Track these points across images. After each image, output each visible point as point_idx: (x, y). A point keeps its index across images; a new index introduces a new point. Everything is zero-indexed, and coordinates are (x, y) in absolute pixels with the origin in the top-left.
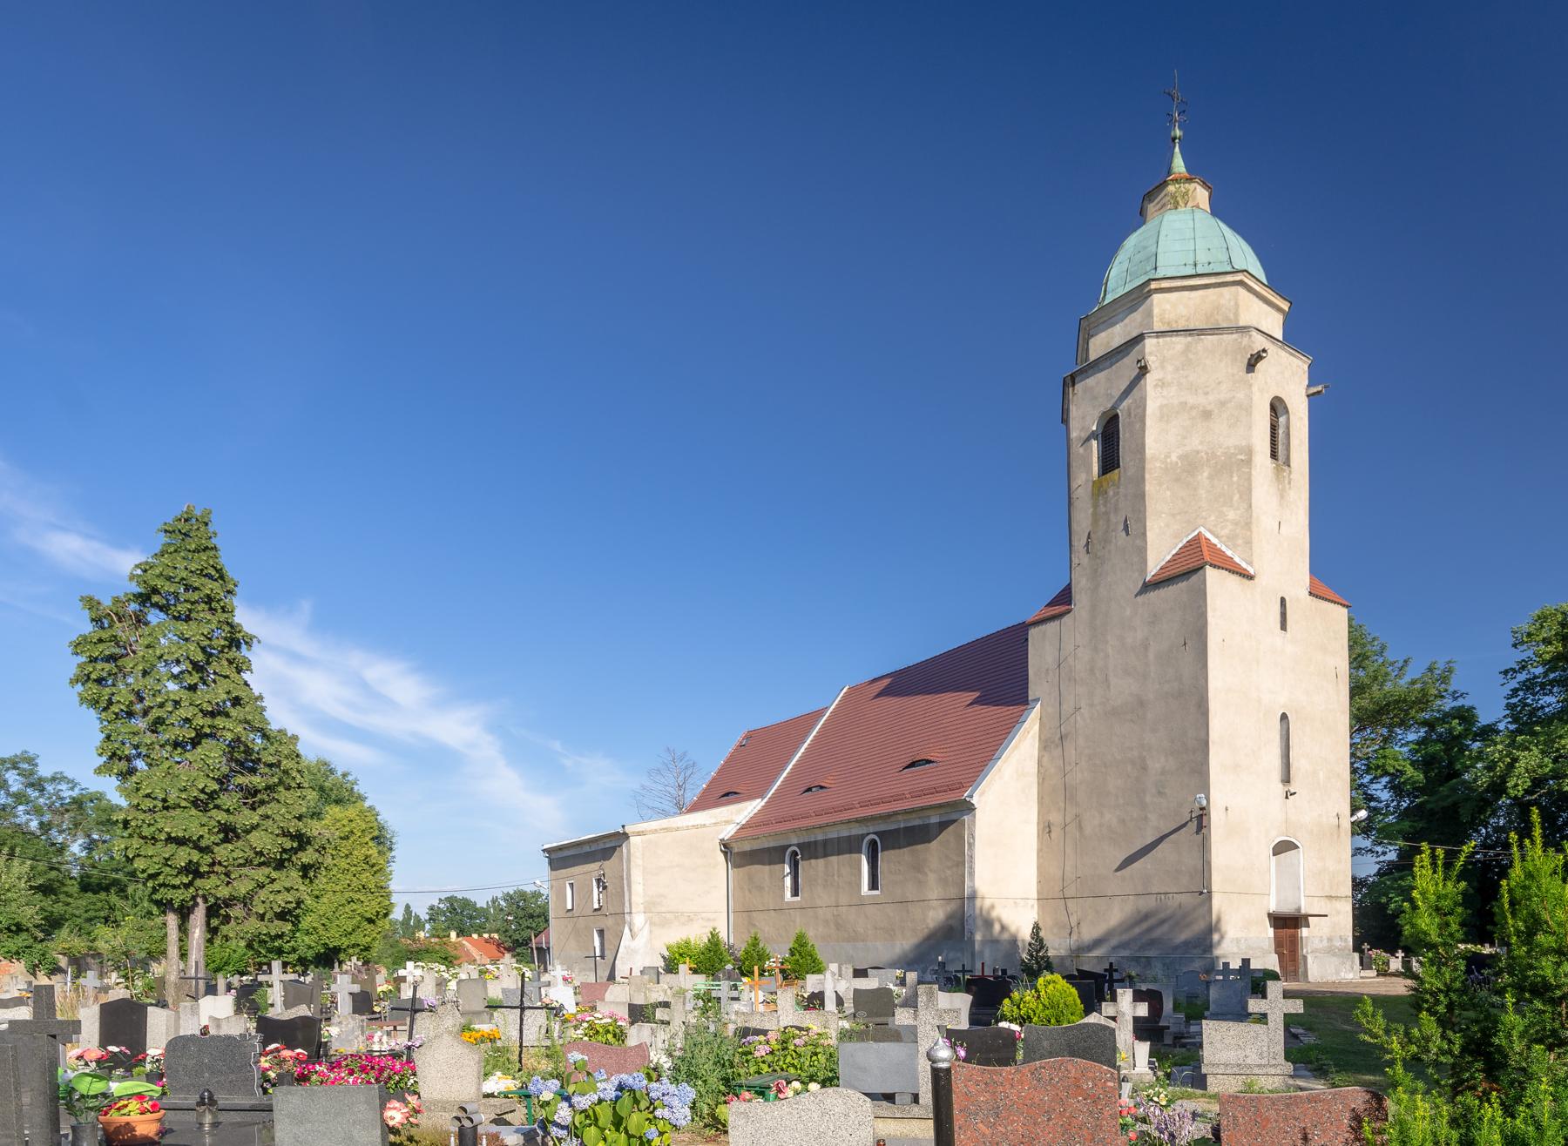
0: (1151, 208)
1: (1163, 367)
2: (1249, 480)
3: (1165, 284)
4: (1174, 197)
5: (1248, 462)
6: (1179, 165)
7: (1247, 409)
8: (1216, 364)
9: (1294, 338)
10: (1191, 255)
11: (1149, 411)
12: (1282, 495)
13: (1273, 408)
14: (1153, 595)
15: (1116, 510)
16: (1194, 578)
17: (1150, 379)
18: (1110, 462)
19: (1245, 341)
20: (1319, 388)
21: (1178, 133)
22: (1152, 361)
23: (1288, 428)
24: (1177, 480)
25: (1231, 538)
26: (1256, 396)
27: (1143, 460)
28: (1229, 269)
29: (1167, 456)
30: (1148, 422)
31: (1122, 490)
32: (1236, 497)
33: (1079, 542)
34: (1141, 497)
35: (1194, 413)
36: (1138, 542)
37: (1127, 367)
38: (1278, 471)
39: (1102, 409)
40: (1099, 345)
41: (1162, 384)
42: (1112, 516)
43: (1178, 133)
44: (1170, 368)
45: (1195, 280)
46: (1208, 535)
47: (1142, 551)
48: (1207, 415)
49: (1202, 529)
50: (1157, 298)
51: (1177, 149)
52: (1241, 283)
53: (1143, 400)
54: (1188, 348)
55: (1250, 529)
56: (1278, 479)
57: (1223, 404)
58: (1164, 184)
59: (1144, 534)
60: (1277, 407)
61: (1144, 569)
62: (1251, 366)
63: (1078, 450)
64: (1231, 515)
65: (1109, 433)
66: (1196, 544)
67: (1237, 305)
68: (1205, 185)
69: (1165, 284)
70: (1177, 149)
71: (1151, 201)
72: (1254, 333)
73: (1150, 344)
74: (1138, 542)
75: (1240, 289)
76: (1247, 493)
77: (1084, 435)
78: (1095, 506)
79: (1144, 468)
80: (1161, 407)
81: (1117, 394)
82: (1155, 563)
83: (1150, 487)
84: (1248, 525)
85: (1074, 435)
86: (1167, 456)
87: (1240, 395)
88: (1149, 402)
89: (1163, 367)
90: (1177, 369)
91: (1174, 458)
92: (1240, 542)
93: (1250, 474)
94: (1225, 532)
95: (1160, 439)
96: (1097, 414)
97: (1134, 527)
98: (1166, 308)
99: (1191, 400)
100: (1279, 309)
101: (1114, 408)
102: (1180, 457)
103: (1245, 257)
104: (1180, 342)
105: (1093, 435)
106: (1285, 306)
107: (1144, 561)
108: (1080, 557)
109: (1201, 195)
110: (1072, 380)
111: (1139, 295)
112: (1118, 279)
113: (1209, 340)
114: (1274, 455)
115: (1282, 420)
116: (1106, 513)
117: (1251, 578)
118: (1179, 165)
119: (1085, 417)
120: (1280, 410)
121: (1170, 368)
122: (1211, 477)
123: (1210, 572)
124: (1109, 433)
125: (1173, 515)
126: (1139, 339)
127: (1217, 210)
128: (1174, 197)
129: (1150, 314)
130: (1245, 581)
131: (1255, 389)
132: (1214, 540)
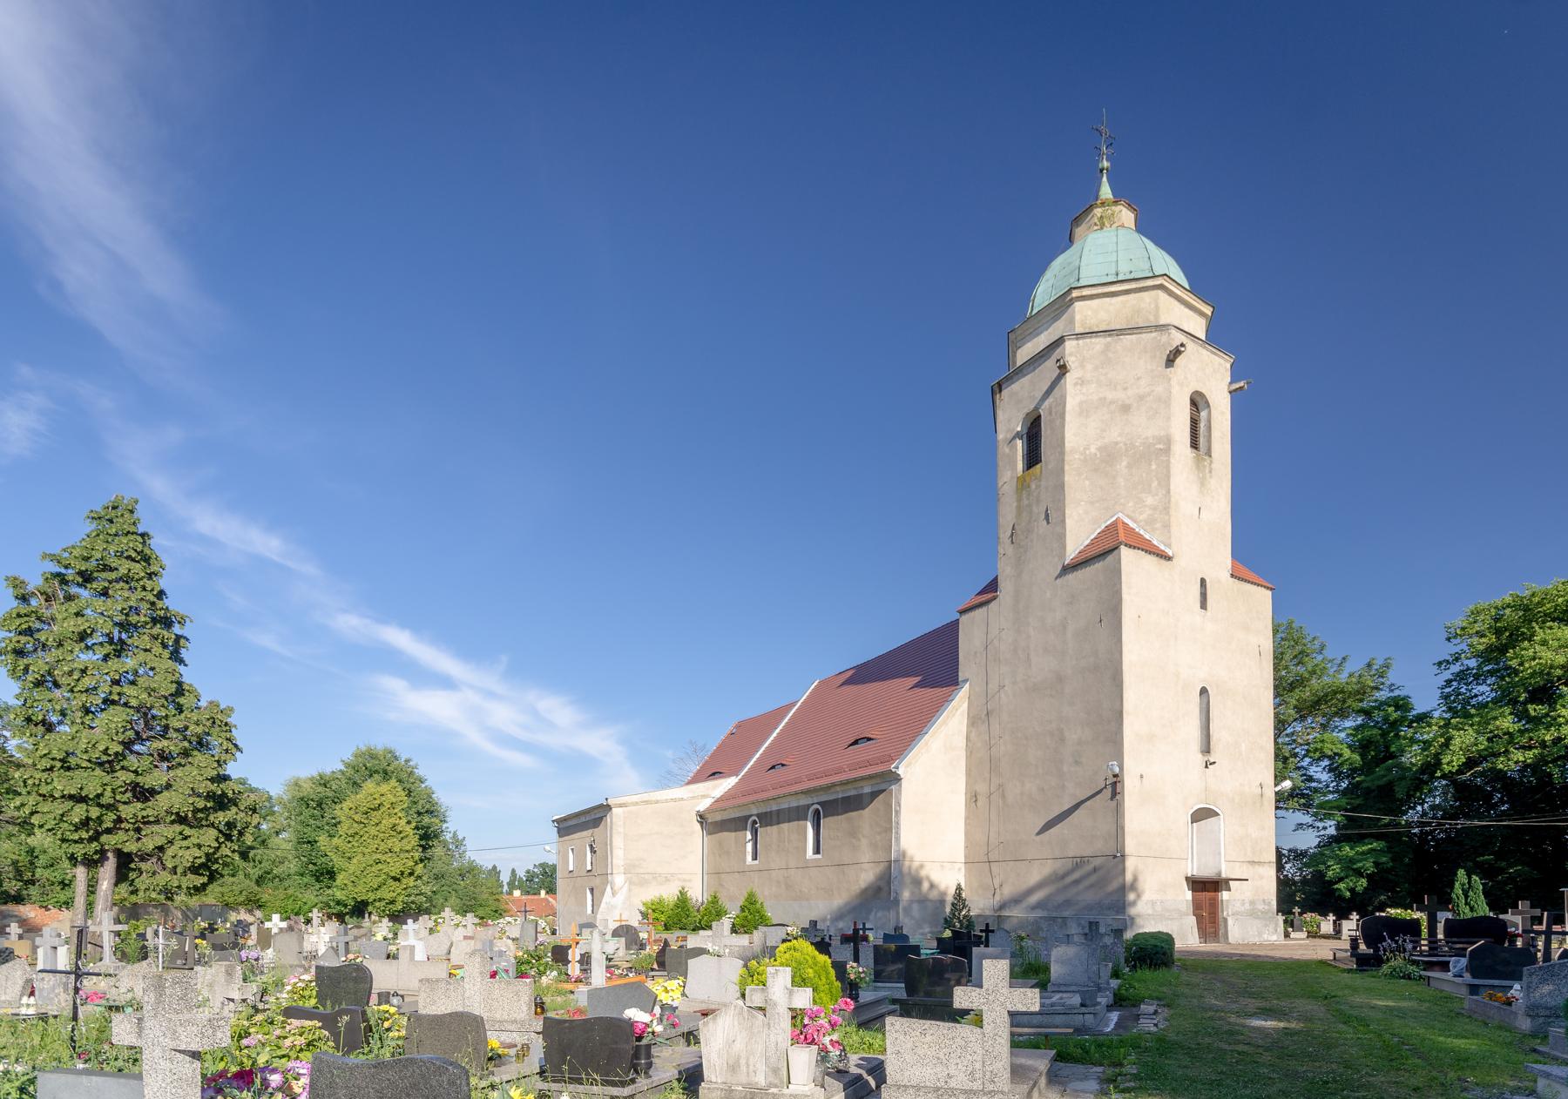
0: (1078, 231)
1: (1082, 366)
2: (1168, 468)
3: (1086, 292)
5: (1167, 451)
6: (1106, 191)
7: (1166, 401)
9: (1216, 338)
11: (1068, 407)
12: (1202, 483)
13: (1193, 403)
14: (1070, 577)
15: (1038, 501)
16: (1110, 558)
17: (1070, 378)
19: (1164, 338)
21: (1106, 164)
22: (1071, 361)
24: (1096, 470)
25: (1150, 522)
26: (1175, 390)
27: (1062, 453)
31: (1043, 483)
32: (1155, 484)
34: (1061, 487)
35: (1113, 407)
37: (1049, 368)
38: (1198, 461)
39: (1026, 411)
40: (1024, 354)
41: (1082, 382)
42: (1035, 509)
44: (1089, 367)
46: (1127, 521)
47: (1061, 538)
48: (1126, 408)
50: (1077, 305)
51: (1105, 179)
52: (1161, 287)
54: (1107, 346)
55: (1168, 513)
56: (1198, 467)
57: (1141, 398)
58: (1091, 208)
59: (1063, 521)
62: (1172, 358)
63: (1004, 449)
64: (1150, 500)
65: (1033, 434)
66: (1112, 529)
67: (1157, 308)
69: (1086, 292)
70: (1105, 179)
72: (1173, 331)
73: (1069, 345)
75: (1160, 293)
77: (1010, 436)
78: (1019, 500)
80: (1081, 403)
81: (1039, 395)
82: (1075, 545)
83: (1068, 478)
84: (1166, 509)
85: (1001, 436)
87: (1160, 389)
88: (1069, 399)
90: (1096, 368)
91: (1093, 450)
96: (1021, 416)
97: (1054, 516)
98: (1085, 313)
99: (1110, 395)
100: (1202, 314)
101: (1036, 408)
102: (1099, 449)
103: (1164, 263)
104: (1099, 343)
105: (1018, 435)
106: (1208, 310)
107: (1064, 547)
109: (1126, 216)
110: (1000, 386)
111: (1063, 303)
112: (1043, 294)
114: (1194, 444)
115: (1203, 414)
116: (1029, 505)
117: (1169, 558)
118: (1106, 191)
119: (1010, 420)
121: (1089, 367)
122: (1129, 466)
123: (1123, 549)
124: (1033, 434)
125: (1092, 503)
126: (1059, 342)
127: (1141, 228)
129: (1072, 321)
131: (1174, 382)
132: (1132, 525)
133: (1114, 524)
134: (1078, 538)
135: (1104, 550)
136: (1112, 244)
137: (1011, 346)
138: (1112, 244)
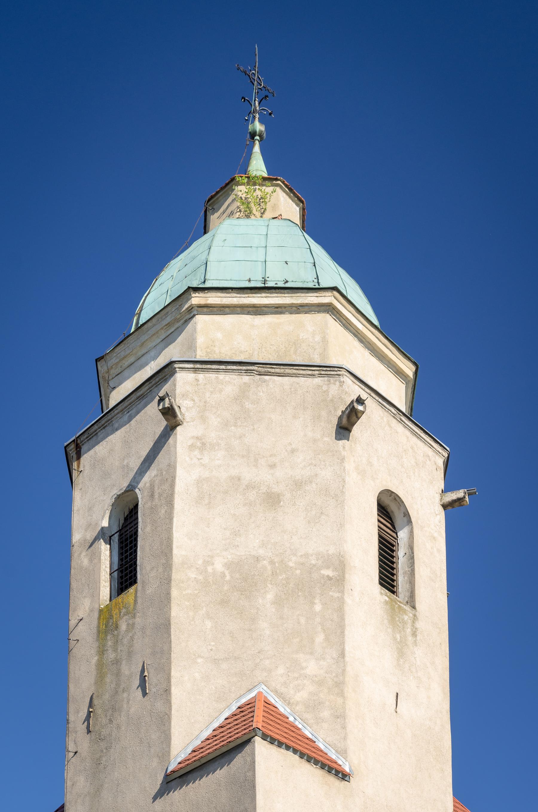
0: (213, 218)
1: (203, 419)
2: (340, 611)
3: (214, 299)
4: (246, 202)
5: (339, 581)
6: (258, 166)
7: (336, 495)
8: (291, 418)
9: (423, 413)
10: (260, 267)
11: (179, 486)
12: (401, 651)
13: (383, 511)
14: (177, 796)
15: (130, 654)
16: (239, 760)
17: (182, 436)
18: (126, 575)
19: (334, 389)
20: (460, 494)
21: (258, 127)
22: (185, 407)
23: (411, 548)
24: (224, 602)
25: (314, 705)
26: (352, 478)
27: (168, 566)
28: (317, 286)
29: (208, 562)
30: (178, 504)
31: (138, 620)
32: (320, 638)
33: (77, 715)
34: (164, 627)
35: (252, 495)
36: (159, 705)
37: (150, 417)
38: (393, 613)
39: (116, 491)
40: (116, 397)
41: (201, 445)
42: (125, 670)
43: (258, 127)
44: (214, 421)
45: (259, 296)
46: (273, 699)
47: (164, 721)
48: (273, 500)
49: (262, 688)
50: (201, 321)
51: (257, 148)
52: (329, 308)
53: (172, 467)
54: (244, 391)
55: (342, 694)
56: (392, 620)
57: (298, 485)
58: (229, 184)
59: (167, 691)
60: (390, 511)
61: (165, 754)
62: (345, 427)
63: (80, 559)
64: (312, 667)
65: (125, 536)
66: (246, 710)
67: (325, 341)
68: (291, 191)
69: (214, 299)
70: (257, 148)
71: (214, 211)
72: (348, 380)
73: (183, 381)
74: (159, 705)
75: (328, 318)
76: (337, 632)
77: (90, 536)
78: (102, 652)
79: (169, 580)
80: (199, 482)
81: (135, 463)
82: (184, 741)
83: (178, 612)
84: (339, 686)
85: (77, 537)
86: (208, 562)
87: (326, 474)
88: (180, 472)
89: (203, 419)
90: (226, 424)
91: (219, 566)
92: (326, 714)
93: (342, 600)
94: (301, 696)
95: (193, 537)
96: (108, 500)
97: (152, 683)
98: (210, 334)
99: (248, 474)
100: (399, 373)
101: (131, 489)
102: (228, 565)
103: (332, 273)
104: (231, 382)
105: (104, 535)
106: (409, 369)
107: (167, 738)
108: (78, 740)
109: (291, 209)
110: (76, 450)
111: (179, 313)
112: (153, 301)
113: (276, 383)
114: (387, 578)
115: (403, 535)
116: (117, 662)
117: (343, 776)
118: (258, 166)
119: (90, 509)
120: (393, 507)
121: (214, 421)
122: (278, 602)
123: (261, 748)
124: (125, 536)
125: (216, 662)
126: (166, 372)
127: (307, 225)
128: (246, 202)
129: (192, 346)
130: (331, 779)
131: (349, 466)
132: (283, 709)
133: (250, 706)
134: (190, 729)
135: (227, 749)
136: (260, 235)
137: (101, 388)
138: (260, 235)
